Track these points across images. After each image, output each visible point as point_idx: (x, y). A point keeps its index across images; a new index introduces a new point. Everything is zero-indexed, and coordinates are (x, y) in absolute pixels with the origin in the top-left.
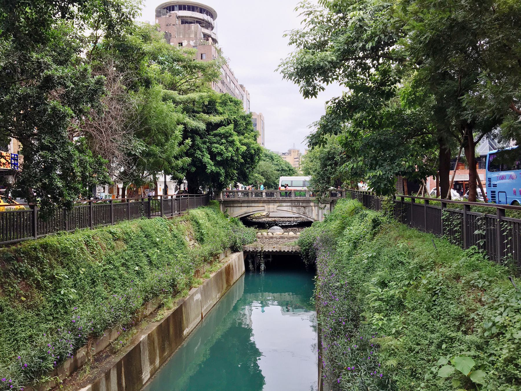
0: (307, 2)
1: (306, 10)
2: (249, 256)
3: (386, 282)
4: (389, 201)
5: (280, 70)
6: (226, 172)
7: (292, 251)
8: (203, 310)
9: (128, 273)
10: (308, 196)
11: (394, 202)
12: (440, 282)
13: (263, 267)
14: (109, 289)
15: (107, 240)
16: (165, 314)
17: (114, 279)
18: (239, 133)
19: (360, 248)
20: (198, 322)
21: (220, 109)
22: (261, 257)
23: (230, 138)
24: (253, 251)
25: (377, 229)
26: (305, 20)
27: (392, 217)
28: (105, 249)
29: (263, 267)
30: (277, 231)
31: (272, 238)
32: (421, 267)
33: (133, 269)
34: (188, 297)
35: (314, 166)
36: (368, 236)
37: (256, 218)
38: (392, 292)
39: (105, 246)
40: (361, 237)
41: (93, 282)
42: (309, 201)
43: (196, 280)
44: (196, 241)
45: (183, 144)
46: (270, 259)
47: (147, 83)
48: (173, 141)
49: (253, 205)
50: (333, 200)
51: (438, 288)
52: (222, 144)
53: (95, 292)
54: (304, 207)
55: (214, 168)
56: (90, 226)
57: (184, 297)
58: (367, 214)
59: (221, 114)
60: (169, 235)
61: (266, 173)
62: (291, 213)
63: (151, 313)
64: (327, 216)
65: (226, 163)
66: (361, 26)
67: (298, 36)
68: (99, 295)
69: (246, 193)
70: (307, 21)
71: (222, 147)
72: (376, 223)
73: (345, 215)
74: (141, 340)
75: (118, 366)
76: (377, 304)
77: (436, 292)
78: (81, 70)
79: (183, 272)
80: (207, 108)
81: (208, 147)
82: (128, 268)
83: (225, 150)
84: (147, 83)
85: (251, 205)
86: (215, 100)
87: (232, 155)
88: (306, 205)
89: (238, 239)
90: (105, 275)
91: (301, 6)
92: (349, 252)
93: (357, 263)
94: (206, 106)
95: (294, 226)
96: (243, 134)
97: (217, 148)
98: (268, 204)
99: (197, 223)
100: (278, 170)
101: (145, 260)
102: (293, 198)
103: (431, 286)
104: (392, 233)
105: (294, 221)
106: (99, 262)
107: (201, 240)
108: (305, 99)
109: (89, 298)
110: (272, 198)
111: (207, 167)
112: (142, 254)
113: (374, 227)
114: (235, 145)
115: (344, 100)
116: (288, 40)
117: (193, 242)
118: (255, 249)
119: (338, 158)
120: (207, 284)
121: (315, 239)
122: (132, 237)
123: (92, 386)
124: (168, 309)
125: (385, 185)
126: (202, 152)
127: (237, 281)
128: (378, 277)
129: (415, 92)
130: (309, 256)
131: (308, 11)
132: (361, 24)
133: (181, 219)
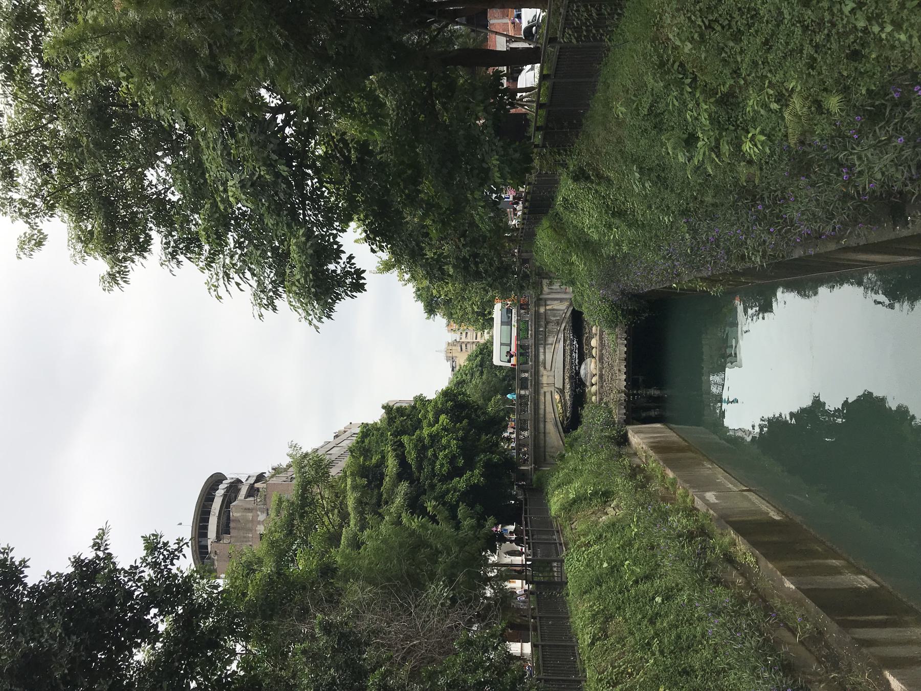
0: (209, 280)
1: (221, 281)
3: (686, 136)
4: (542, 157)
5: (318, 324)
6: (484, 451)
8: (735, 489)
9: (666, 615)
11: (544, 146)
12: (689, 18)
13: (654, 392)
14: (697, 646)
15: (606, 650)
16: (742, 549)
17: (679, 637)
18: (418, 425)
19: (623, 203)
20: (757, 496)
21: (375, 459)
22: (635, 395)
23: (426, 442)
25: (591, 173)
26: (238, 284)
27: (570, 151)
28: (624, 653)
29: (654, 392)
30: (590, 367)
31: (601, 376)
32: (662, 64)
33: (660, 606)
34: (711, 512)
35: (477, 293)
36: (602, 189)
37: (565, 411)
38: (704, 119)
39: (617, 653)
40: (604, 203)
41: (687, 672)
42: (537, 315)
43: (680, 500)
44: (608, 504)
45: (435, 516)
46: (641, 378)
47: (327, 571)
48: (429, 532)
49: (542, 412)
51: (699, 22)
52: (435, 456)
53: (704, 670)
54: (547, 323)
55: (477, 471)
56: (579, 682)
57: (711, 519)
58: (564, 198)
59: (383, 457)
60: (596, 547)
61: (486, 393)
62: (557, 345)
63: (743, 575)
65: (469, 450)
66: (253, 185)
67: (262, 296)
68: (709, 662)
69: (521, 427)
70: (239, 281)
71: (441, 455)
72: (580, 176)
73: (562, 246)
74: (794, 587)
75: (845, 625)
76: (725, 148)
77: (707, 23)
78: (304, 660)
79: (665, 520)
80: (372, 482)
81: (439, 481)
82: (657, 614)
83: (447, 450)
84: (327, 571)
86: (360, 465)
87: (454, 439)
89: (603, 434)
90: (672, 652)
91: (215, 291)
92: (630, 226)
93: (650, 207)
94: (370, 483)
95: (580, 342)
96: (420, 421)
97: (441, 465)
99: (574, 501)
100: (482, 373)
101: (642, 587)
102: (531, 342)
103: (696, 36)
104: (597, 141)
105: (572, 345)
106: (647, 662)
107: (606, 496)
108: (365, 290)
109: (716, 680)
111: (474, 483)
112: (633, 591)
113: (587, 178)
114: (438, 433)
115: (371, 224)
116: (268, 313)
117: (610, 510)
118: (621, 404)
120: (686, 481)
121: (604, 299)
122: (601, 607)
123: (889, 667)
124: (735, 544)
125: (515, 151)
126: (448, 491)
127: (680, 437)
128: (678, 151)
129: (362, 114)
130: (634, 309)
131: (223, 277)
132: (250, 183)
133: (568, 529)
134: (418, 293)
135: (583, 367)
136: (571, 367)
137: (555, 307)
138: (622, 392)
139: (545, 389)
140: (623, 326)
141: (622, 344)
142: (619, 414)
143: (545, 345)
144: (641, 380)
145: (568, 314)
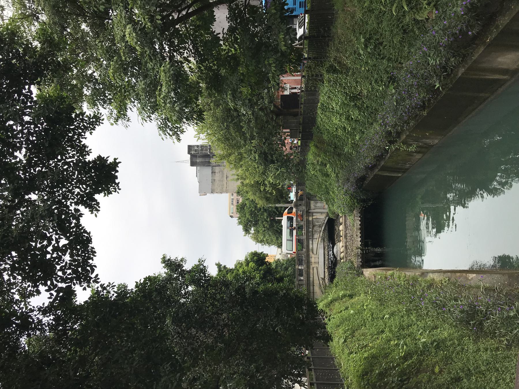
2: (367, 264)
7: (360, 217)
10: (302, 223)
13: (378, 250)
29: (378, 250)
31: (346, 247)
42: (308, 221)
49: (311, 279)
50: (307, 198)
54: (314, 226)
88: (312, 224)
98: (311, 263)
99: (331, 302)
102: (304, 237)
110: (304, 259)
118: (358, 256)
119: (265, 148)
135: (335, 247)
136: (329, 262)
139: (313, 265)
141: (358, 219)
142: (357, 262)
143: (313, 239)
144: (369, 243)
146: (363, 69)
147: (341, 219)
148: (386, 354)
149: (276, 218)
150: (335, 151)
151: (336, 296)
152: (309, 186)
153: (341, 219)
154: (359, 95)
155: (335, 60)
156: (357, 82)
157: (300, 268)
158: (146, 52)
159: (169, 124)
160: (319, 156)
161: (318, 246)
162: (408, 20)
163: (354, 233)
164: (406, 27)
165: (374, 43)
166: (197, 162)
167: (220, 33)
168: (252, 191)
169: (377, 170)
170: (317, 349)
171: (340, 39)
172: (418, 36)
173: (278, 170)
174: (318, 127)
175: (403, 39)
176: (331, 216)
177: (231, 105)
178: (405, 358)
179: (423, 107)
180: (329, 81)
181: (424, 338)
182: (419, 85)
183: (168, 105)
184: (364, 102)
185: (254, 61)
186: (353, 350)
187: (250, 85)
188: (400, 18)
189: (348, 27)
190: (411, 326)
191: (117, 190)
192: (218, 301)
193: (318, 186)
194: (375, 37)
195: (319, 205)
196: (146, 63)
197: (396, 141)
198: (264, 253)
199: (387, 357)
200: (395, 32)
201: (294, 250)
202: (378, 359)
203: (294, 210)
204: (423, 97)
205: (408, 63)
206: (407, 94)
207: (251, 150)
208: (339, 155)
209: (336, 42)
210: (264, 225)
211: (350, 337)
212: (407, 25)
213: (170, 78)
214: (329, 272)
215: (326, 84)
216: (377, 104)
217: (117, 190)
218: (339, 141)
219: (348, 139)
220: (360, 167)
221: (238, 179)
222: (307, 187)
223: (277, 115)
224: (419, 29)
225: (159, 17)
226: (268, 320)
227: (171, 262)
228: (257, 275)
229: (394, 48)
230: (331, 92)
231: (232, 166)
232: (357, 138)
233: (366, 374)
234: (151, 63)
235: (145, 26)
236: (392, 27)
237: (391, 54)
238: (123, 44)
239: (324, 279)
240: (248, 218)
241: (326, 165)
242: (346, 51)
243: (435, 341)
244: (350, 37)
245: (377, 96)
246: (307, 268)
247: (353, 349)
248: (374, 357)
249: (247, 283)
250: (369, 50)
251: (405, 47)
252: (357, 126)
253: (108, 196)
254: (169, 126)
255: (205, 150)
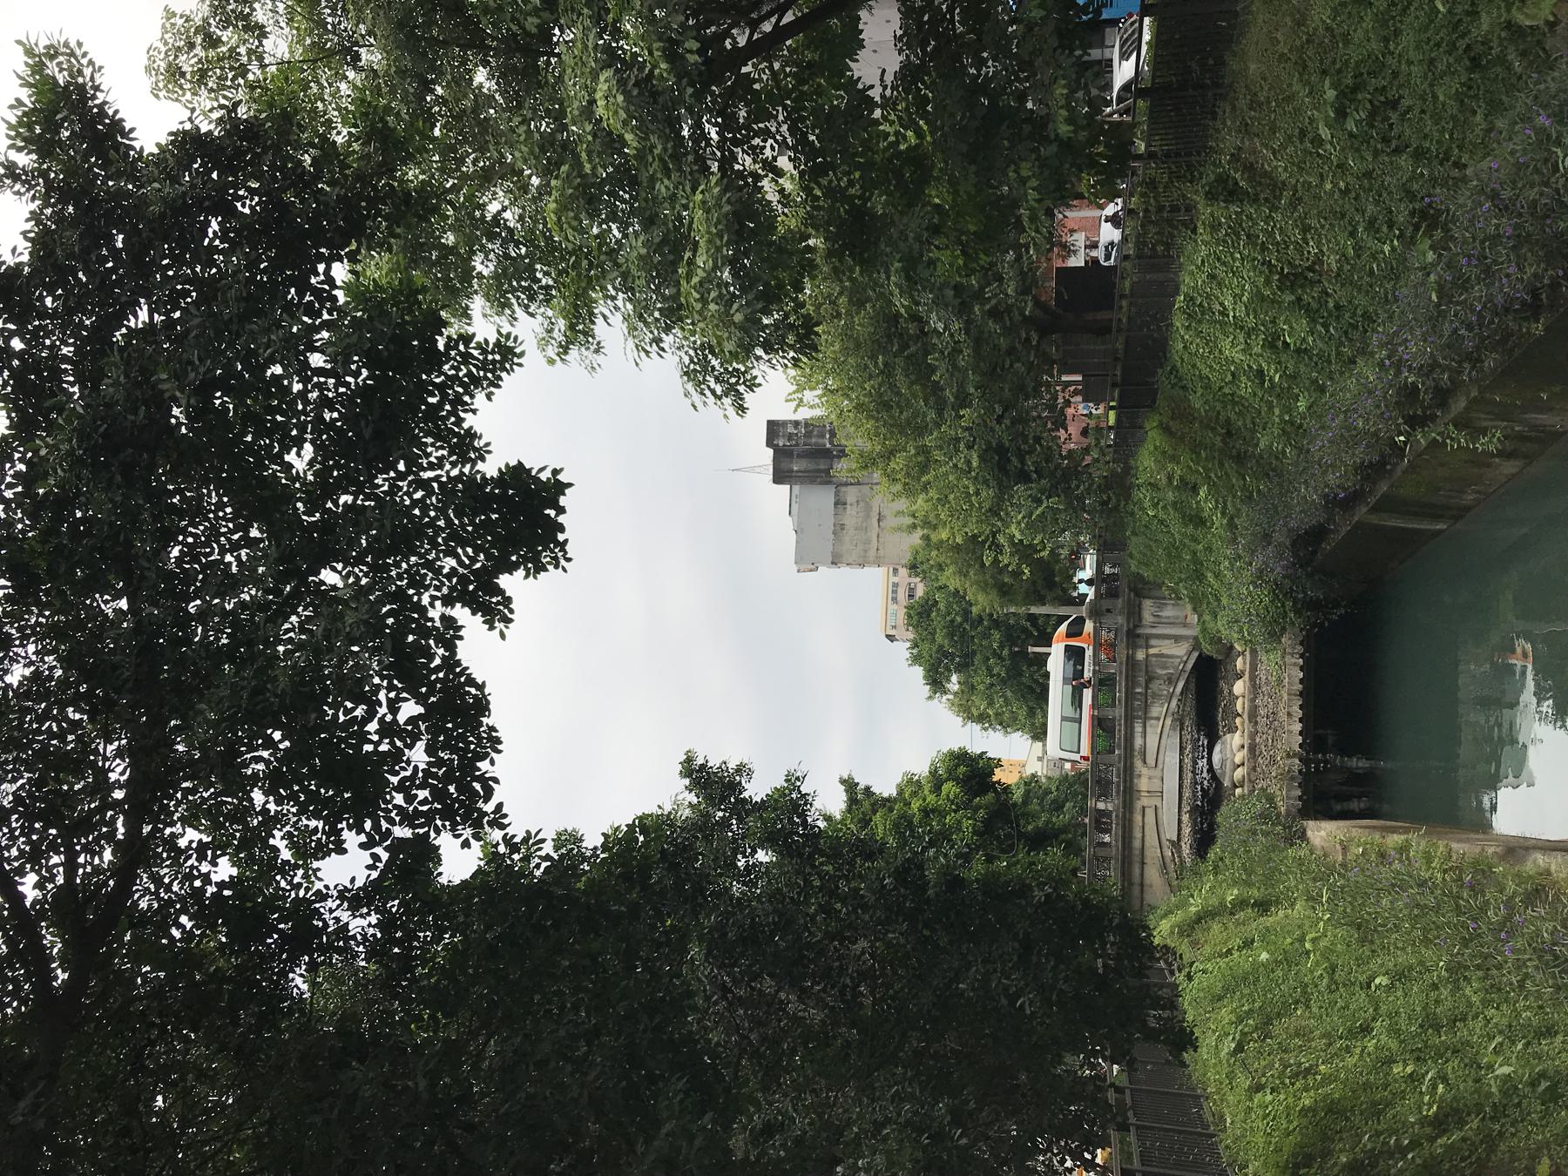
7: (1302, 656)
13: (1358, 763)
22: (1321, 761)
24: (1300, 785)
29: (1358, 763)
31: (1253, 748)
42: (1131, 663)
49: (1137, 844)
50: (1130, 590)
54: (1150, 679)
64: (1183, 576)
85: (1137, 852)
98: (1135, 795)
99: (1199, 919)
102: (1119, 712)
110: (1115, 779)
118: (1293, 779)
119: (1002, 433)
134: (915, 651)
135: (1217, 748)
136: (1194, 793)
137: (1165, 651)
138: (1295, 755)
139: (1144, 801)
140: (1297, 630)
141: (1295, 664)
143: (1145, 719)
144: (1330, 740)
145: (1190, 665)
146: (1328, 186)
147: (1239, 662)
148: (1375, 1104)
149: (1030, 649)
150: (1225, 444)
151: (1214, 901)
152: (1140, 552)
153: (1240, 659)
154: (1310, 269)
155: (1235, 158)
156: (1306, 229)
157: (1101, 806)
158: (653, 147)
159: (715, 362)
160: (1174, 459)
161: (1163, 741)
162: (1485, 27)
163: (1282, 705)
164: (1479, 49)
165: (1370, 101)
166: (792, 471)
167: (872, 87)
168: (956, 564)
169: (1364, 510)
170: (1148, 1063)
171: (1255, 94)
172: (1520, 78)
173: (1039, 502)
174: (1174, 368)
175: (1470, 88)
176: (1208, 649)
177: (900, 303)
178: (1440, 1124)
179: (1533, 308)
180: (1212, 227)
181: (1507, 1062)
182: (1519, 236)
183: (712, 307)
184: (1327, 294)
185: (973, 168)
186: (1264, 1079)
187: (961, 243)
188: (1460, 20)
189: (1282, 55)
190: (1464, 1019)
191: (563, 562)
192: (844, 901)
193: (1169, 555)
194: (1374, 82)
195: (1169, 612)
196: (652, 180)
197: (1433, 418)
198: (989, 755)
199: (1379, 1113)
200: (1441, 67)
201: (1085, 750)
202: (1347, 1119)
203: (1089, 626)
204: (1535, 275)
205: (1484, 165)
206: (1476, 266)
207: (958, 440)
208: (1240, 459)
209: (1242, 103)
210: (989, 669)
211: (1255, 1035)
212: (1483, 43)
213: (720, 227)
214: (1194, 824)
215: (1203, 233)
216: (1373, 298)
217: (563, 562)
218: (1240, 414)
219: (1271, 407)
220: (1306, 498)
221: (914, 526)
222: (1131, 555)
223: (1044, 332)
224: (1523, 54)
225: (693, 45)
226: (995, 971)
227: (708, 773)
228: (967, 823)
229: (1437, 119)
230: (1219, 259)
231: (898, 487)
232: (1302, 405)
233: (1308, 1160)
234: (666, 182)
235: (651, 71)
236: (1431, 51)
237: (1426, 136)
238: (589, 128)
239: (1176, 845)
240: (941, 647)
241: (1195, 490)
242: (1273, 130)
243: (1543, 1075)
244: (1290, 85)
245: (1371, 273)
246: (1124, 807)
247: (1264, 1075)
248: (1334, 1109)
249: (932, 852)
250: (1351, 125)
251: (1475, 113)
252: (1302, 369)
253: (535, 578)
254: (713, 368)
255: (818, 436)
